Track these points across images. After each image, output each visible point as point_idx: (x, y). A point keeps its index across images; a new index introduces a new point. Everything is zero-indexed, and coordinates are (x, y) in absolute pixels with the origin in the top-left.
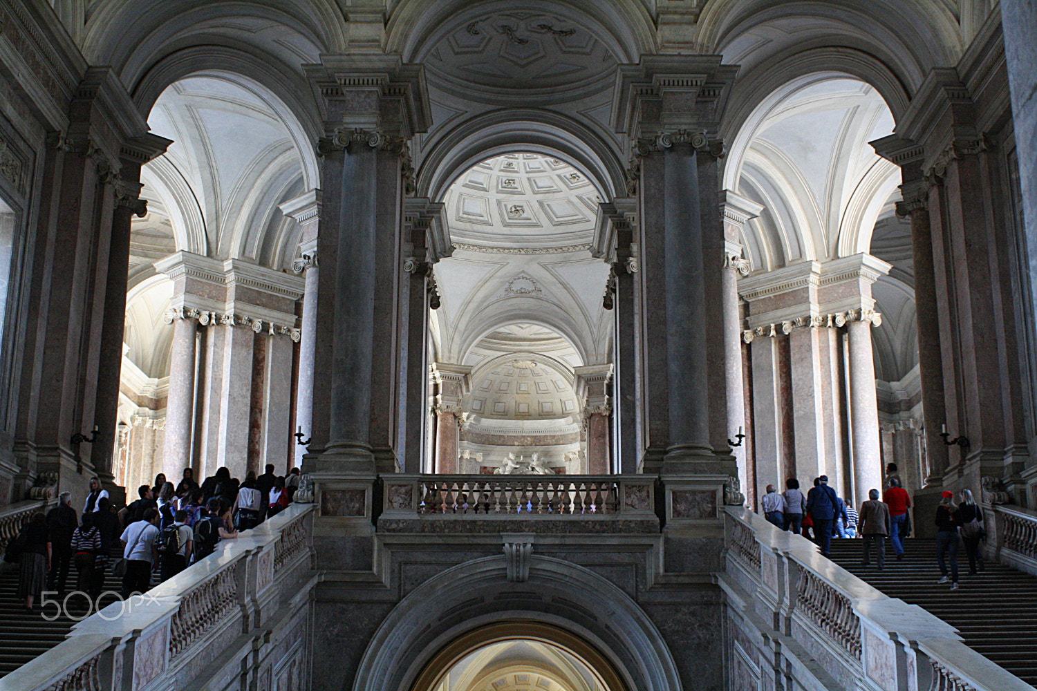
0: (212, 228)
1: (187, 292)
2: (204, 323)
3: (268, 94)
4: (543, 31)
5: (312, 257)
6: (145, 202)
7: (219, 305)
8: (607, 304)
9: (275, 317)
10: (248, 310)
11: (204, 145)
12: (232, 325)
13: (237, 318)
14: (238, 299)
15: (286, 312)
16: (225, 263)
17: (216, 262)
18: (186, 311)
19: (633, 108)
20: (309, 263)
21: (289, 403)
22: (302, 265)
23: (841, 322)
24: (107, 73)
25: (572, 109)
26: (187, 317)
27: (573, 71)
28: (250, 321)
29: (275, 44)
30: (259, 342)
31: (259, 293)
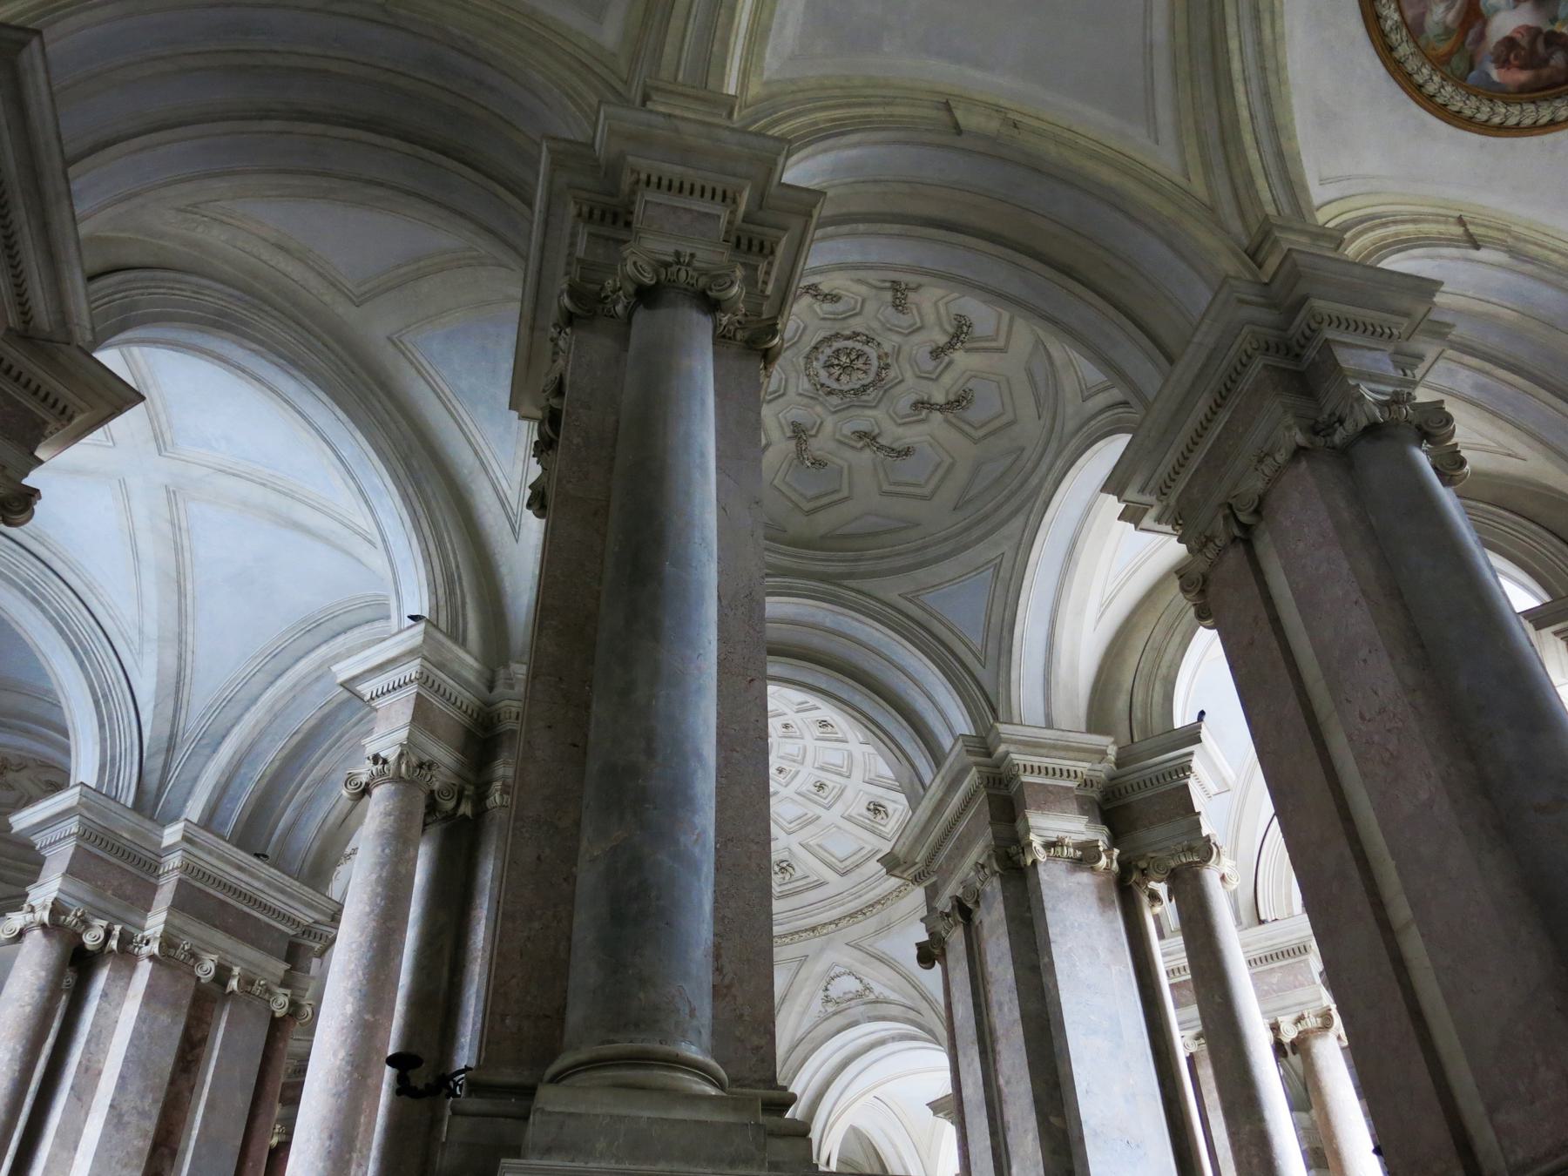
0: (155, 765)
1: (71, 872)
2: (91, 940)
3: (355, 445)
4: (861, 444)
5: (392, 758)
6: (33, 494)
7: (135, 919)
8: (928, 955)
9: (245, 959)
10: (195, 932)
11: (181, 594)
12: (152, 957)
13: (168, 942)
14: (177, 906)
15: (270, 952)
16: (167, 831)
17: (148, 824)
18: (57, 909)
19: (1218, 404)
20: (382, 773)
21: (239, 1142)
22: (364, 779)
23: (1289, 1034)
24: (23, 44)
25: (892, 590)
26: (54, 927)
27: (890, 531)
28: (193, 955)
29: (390, 349)
30: (202, 1005)
31: (223, 903)
